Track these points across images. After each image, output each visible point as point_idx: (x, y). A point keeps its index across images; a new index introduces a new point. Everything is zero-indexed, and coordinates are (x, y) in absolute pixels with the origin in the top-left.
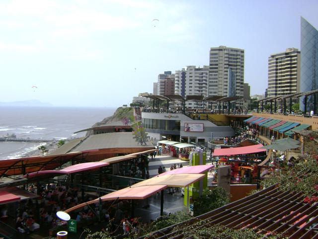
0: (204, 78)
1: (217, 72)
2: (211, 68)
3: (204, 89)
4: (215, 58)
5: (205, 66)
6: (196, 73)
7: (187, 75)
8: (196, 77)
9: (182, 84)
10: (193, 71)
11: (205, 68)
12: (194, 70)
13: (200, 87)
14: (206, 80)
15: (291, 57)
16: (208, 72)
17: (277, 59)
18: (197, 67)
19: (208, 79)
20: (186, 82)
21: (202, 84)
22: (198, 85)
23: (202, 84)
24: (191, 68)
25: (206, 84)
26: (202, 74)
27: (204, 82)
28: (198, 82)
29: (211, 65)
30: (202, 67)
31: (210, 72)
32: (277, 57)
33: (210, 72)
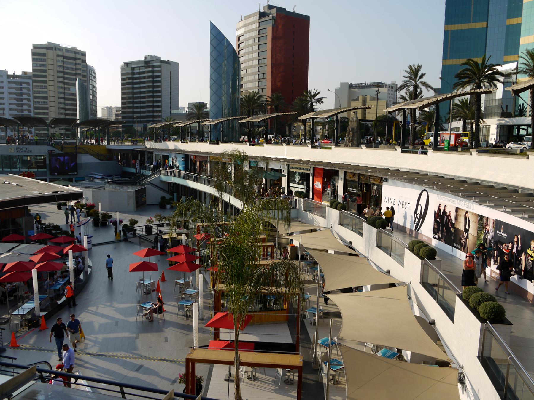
2: (35, 76)
3: (25, 107)
4: (41, 60)
5: (25, 73)
8: (9, 88)
15: (153, 67)
16: (30, 81)
17: (133, 69)
18: (10, 73)
19: (31, 93)
22: (15, 102)
26: (21, 83)
28: (14, 96)
30: (19, 73)
31: (34, 81)
32: (133, 66)
33: (34, 81)
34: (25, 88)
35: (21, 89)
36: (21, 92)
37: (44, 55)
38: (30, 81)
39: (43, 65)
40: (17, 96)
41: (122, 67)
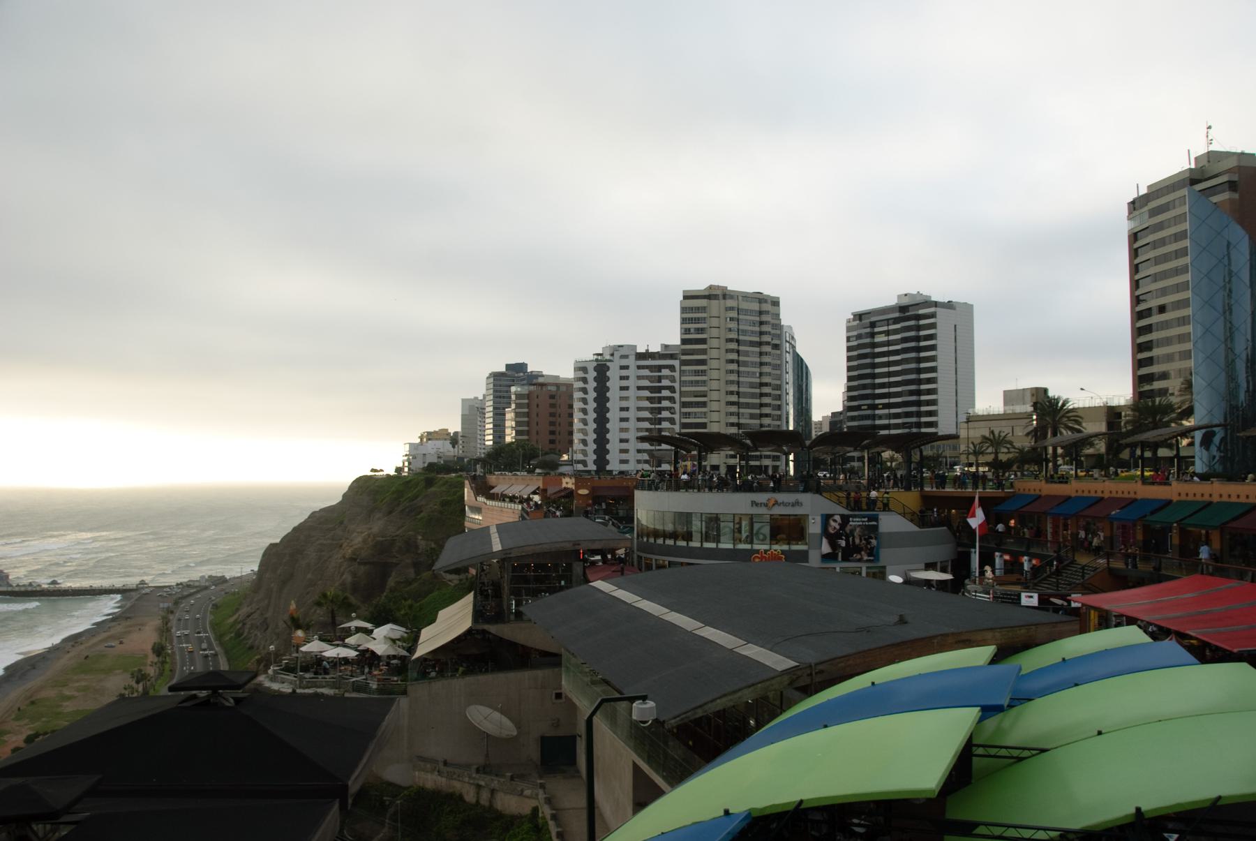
0: (665, 383)
1: (703, 362)
2: (685, 353)
5: (666, 347)
6: (639, 367)
7: (613, 374)
8: (639, 378)
9: (595, 379)
10: (631, 362)
11: (667, 353)
12: (632, 358)
13: (652, 410)
14: (672, 389)
17: (873, 325)
18: (641, 349)
20: (608, 394)
21: (660, 400)
22: (647, 404)
23: (660, 400)
24: (623, 352)
25: (672, 399)
26: (660, 368)
27: (666, 393)
28: (647, 393)
29: (684, 341)
30: (655, 348)
32: (873, 319)
33: (684, 363)
34: (666, 377)
35: (659, 379)
36: (659, 374)
37: (703, 309)
38: (676, 363)
39: (701, 331)
40: (651, 393)
41: (849, 321)
